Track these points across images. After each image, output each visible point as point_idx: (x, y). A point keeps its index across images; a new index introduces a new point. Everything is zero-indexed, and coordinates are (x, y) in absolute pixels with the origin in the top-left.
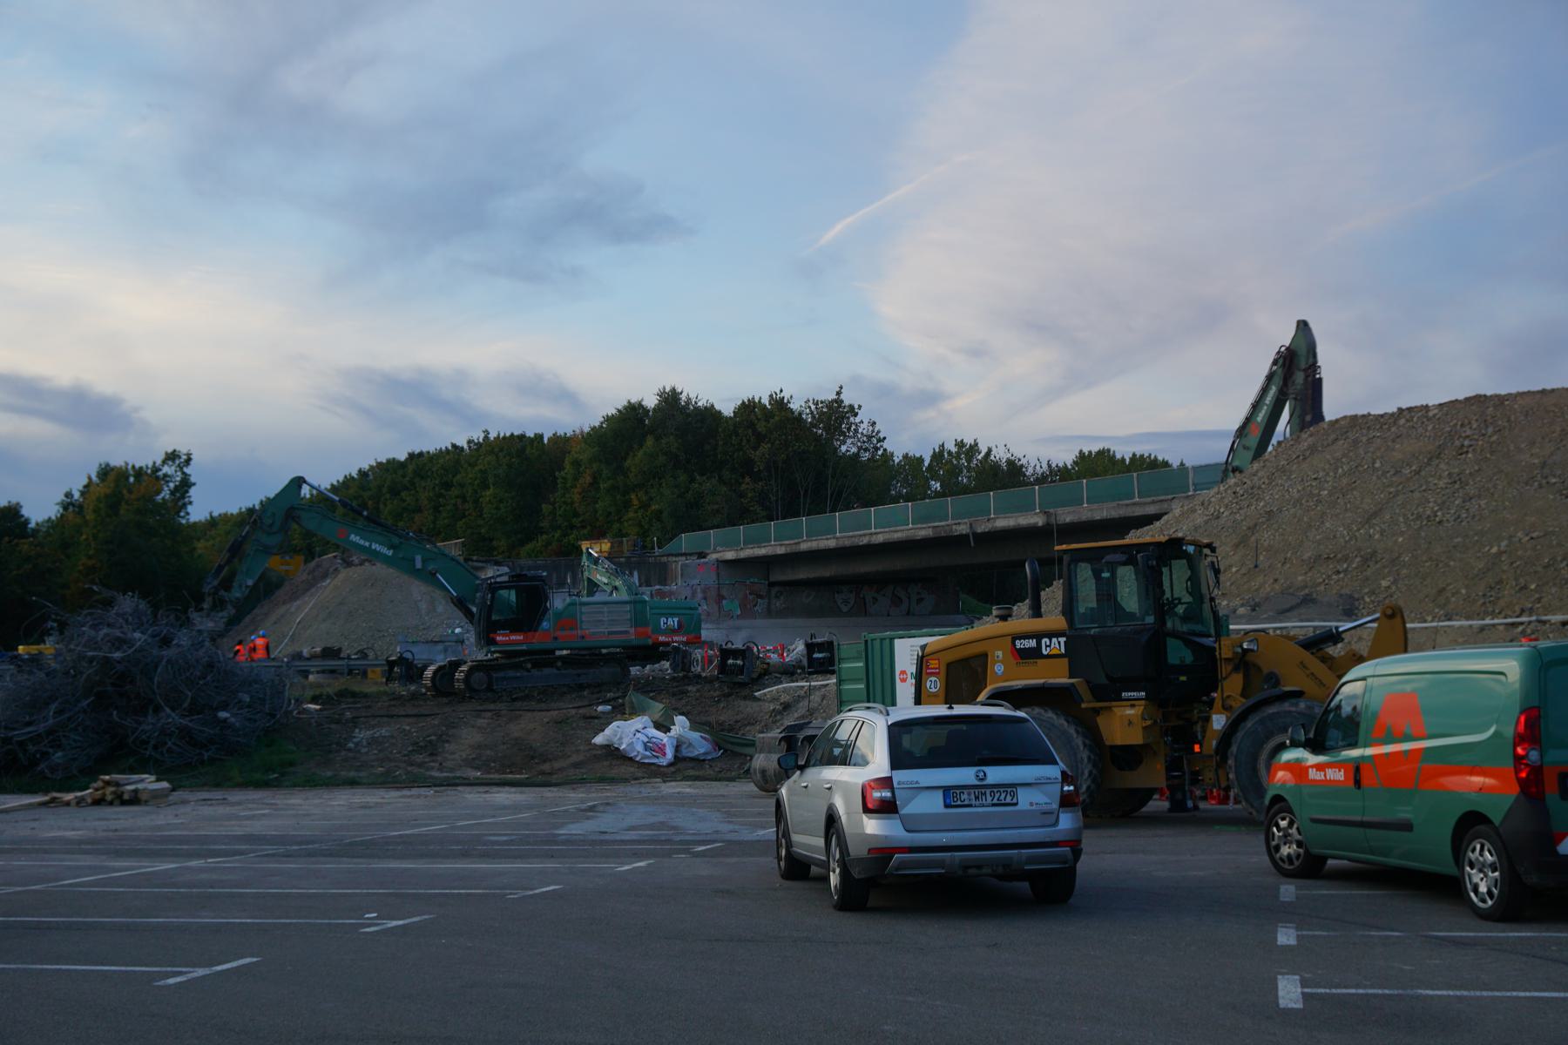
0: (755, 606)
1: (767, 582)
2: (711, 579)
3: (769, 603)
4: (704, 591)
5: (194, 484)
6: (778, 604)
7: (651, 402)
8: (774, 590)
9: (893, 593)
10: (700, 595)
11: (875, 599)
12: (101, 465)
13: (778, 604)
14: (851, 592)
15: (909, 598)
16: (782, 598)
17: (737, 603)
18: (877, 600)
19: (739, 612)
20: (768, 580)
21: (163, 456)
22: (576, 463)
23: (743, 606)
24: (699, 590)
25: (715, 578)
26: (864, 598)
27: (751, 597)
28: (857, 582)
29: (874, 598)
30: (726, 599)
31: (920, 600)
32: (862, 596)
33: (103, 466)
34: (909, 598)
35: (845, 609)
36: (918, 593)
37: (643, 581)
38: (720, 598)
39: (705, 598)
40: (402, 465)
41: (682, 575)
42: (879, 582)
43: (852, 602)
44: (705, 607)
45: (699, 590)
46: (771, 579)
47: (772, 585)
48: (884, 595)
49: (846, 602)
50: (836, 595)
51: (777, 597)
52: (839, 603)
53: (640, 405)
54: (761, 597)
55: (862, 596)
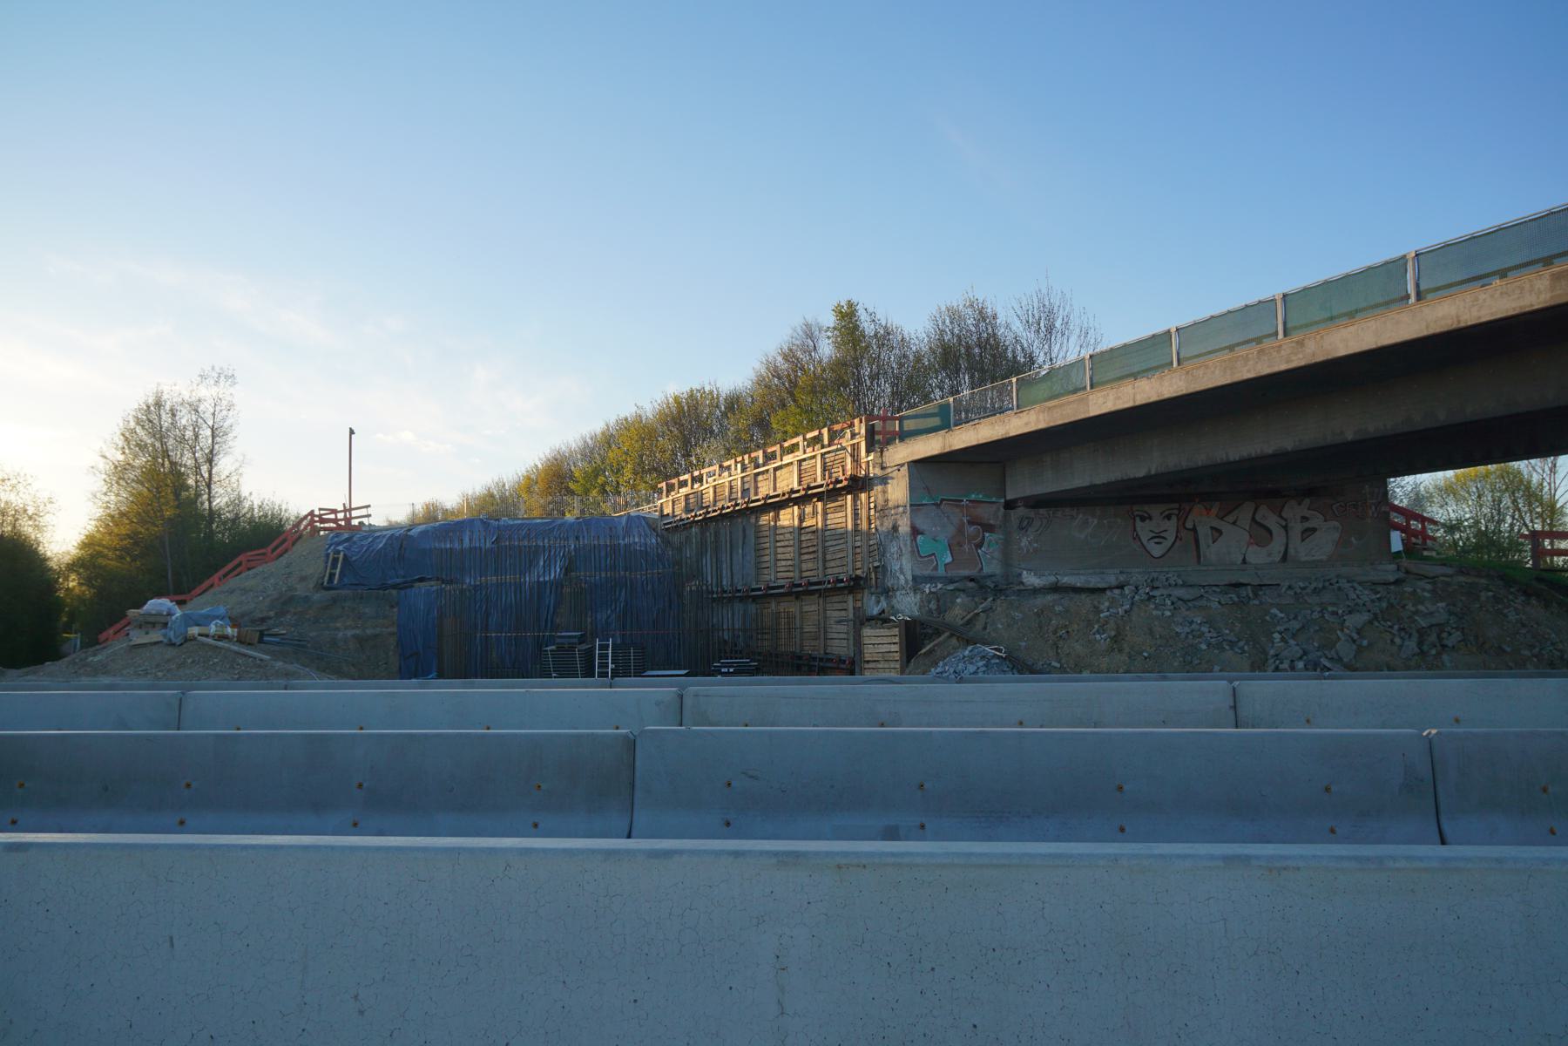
0: (979, 546)
1: (1003, 501)
8: (1015, 515)
9: (1253, 519)
11: (1218, 532)
14: (1169, 517)
18: (1220, 532)
20: (1005, 497)
26: (1194, 530)
29: (1212, 528)
30: (922, 533)
31: (1308, 532)
32: (1189, 525)
34: (1285, 528)
35: (1157, 551)
36: (1304, 519)
47: (1010, 505)
49: (1158, 537)
50: (1139, 523)
51: (1021, 528)
52: (1144, 540)
54: (989, 528)
55: (1189, 525)
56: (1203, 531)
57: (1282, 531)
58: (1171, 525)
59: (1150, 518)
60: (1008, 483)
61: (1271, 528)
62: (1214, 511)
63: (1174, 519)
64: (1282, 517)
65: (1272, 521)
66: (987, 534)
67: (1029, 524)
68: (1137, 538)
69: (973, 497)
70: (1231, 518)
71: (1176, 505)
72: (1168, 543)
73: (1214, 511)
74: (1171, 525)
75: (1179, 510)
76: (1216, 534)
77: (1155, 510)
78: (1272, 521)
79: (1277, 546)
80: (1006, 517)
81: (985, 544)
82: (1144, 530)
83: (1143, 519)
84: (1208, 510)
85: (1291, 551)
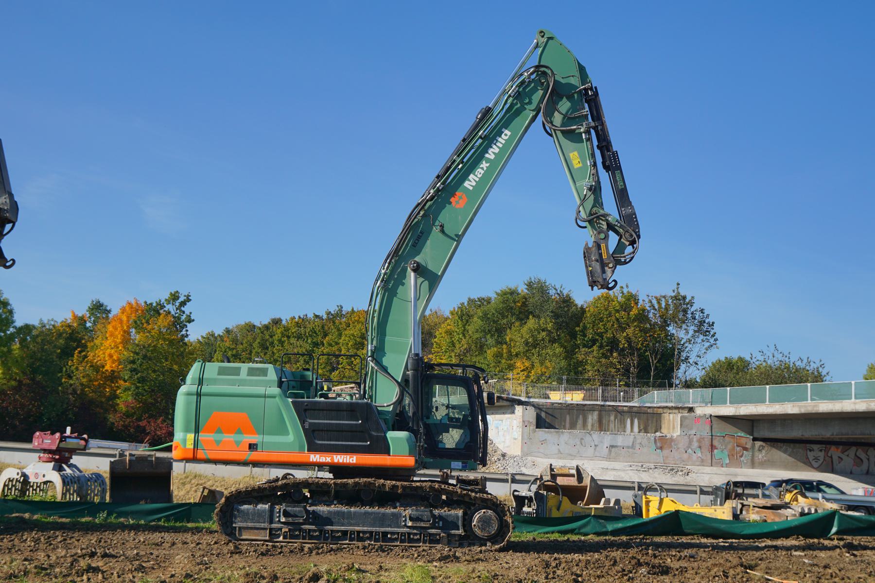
0: (741, 456)
1: (752, 437)
2: (706, 431)
3: (753, 456)
4: (699, 441)
5: (193, 320)
6: (760, 456)
7: (522, 289)
9: (856, 455)
10: (695, 444)
12: (93, 301)
13: (760, 456)
14: (821, 451)
15: (868, 459)
16: (764, 451)
17: (726, 452)
18: (842, 459)
19: (727, 461)
21: (167, 296)
22: (449, 333)
23: (731, 456)
24: (695, 440)
25: (708, 428)
26: (831, 457)
27: (738, 449)
28: (827, 443)
29: (839, 457)
30: (717, 449)
32: (829, 455)
33: (94, 303)
34: (868, 459)
37: (642, 427)
38: (712, 447)
39: (700, 447)
40: (267, 327)
41: (681, 425)
42: (846, 444)
43: (822, 460)
44: (700, 455)
45: (695, 440)
46: (756, 435)
48: (848, 456)
49: (816, 459)
50: (809, 453)
51: (759, 450)
52: (811, 460)
53: (512, 293)
54: (745, 449)
55: (829, 455)
56: (835, 458)
57: (867, 461)
58: (822, 454)
59: (813, 450)
60: (755, 429)
61: (863, 459)
62: (840, 450)
63: (823, 452)
64: (867, 455)
65: (862, 455)
66: (745, 452)
67: (763, 449)
68: (808, 458)
69: (739, 434)
70: (846, 453)
71: (824, 446)
72: (820, 462)
73: (840, 450)
74: (822, 454)
75: (826, 448)
76: (840, 460)
77: (816, 447)
78: (862, 455)
79: (864, 467)
80: (753, 446)
81: (744, 455)
82: (811, 455)
83: (810, 451)
84: (837, 448)
85: (871, 470)
